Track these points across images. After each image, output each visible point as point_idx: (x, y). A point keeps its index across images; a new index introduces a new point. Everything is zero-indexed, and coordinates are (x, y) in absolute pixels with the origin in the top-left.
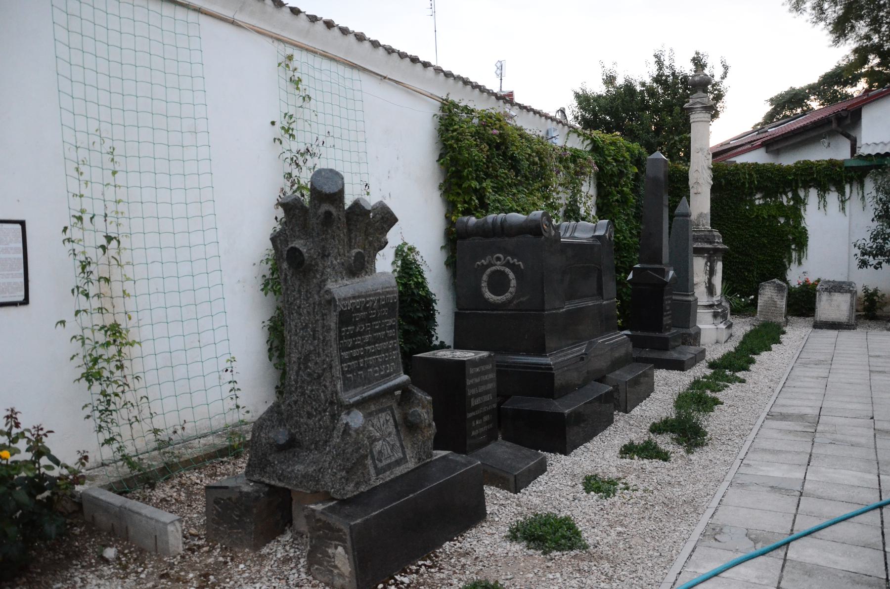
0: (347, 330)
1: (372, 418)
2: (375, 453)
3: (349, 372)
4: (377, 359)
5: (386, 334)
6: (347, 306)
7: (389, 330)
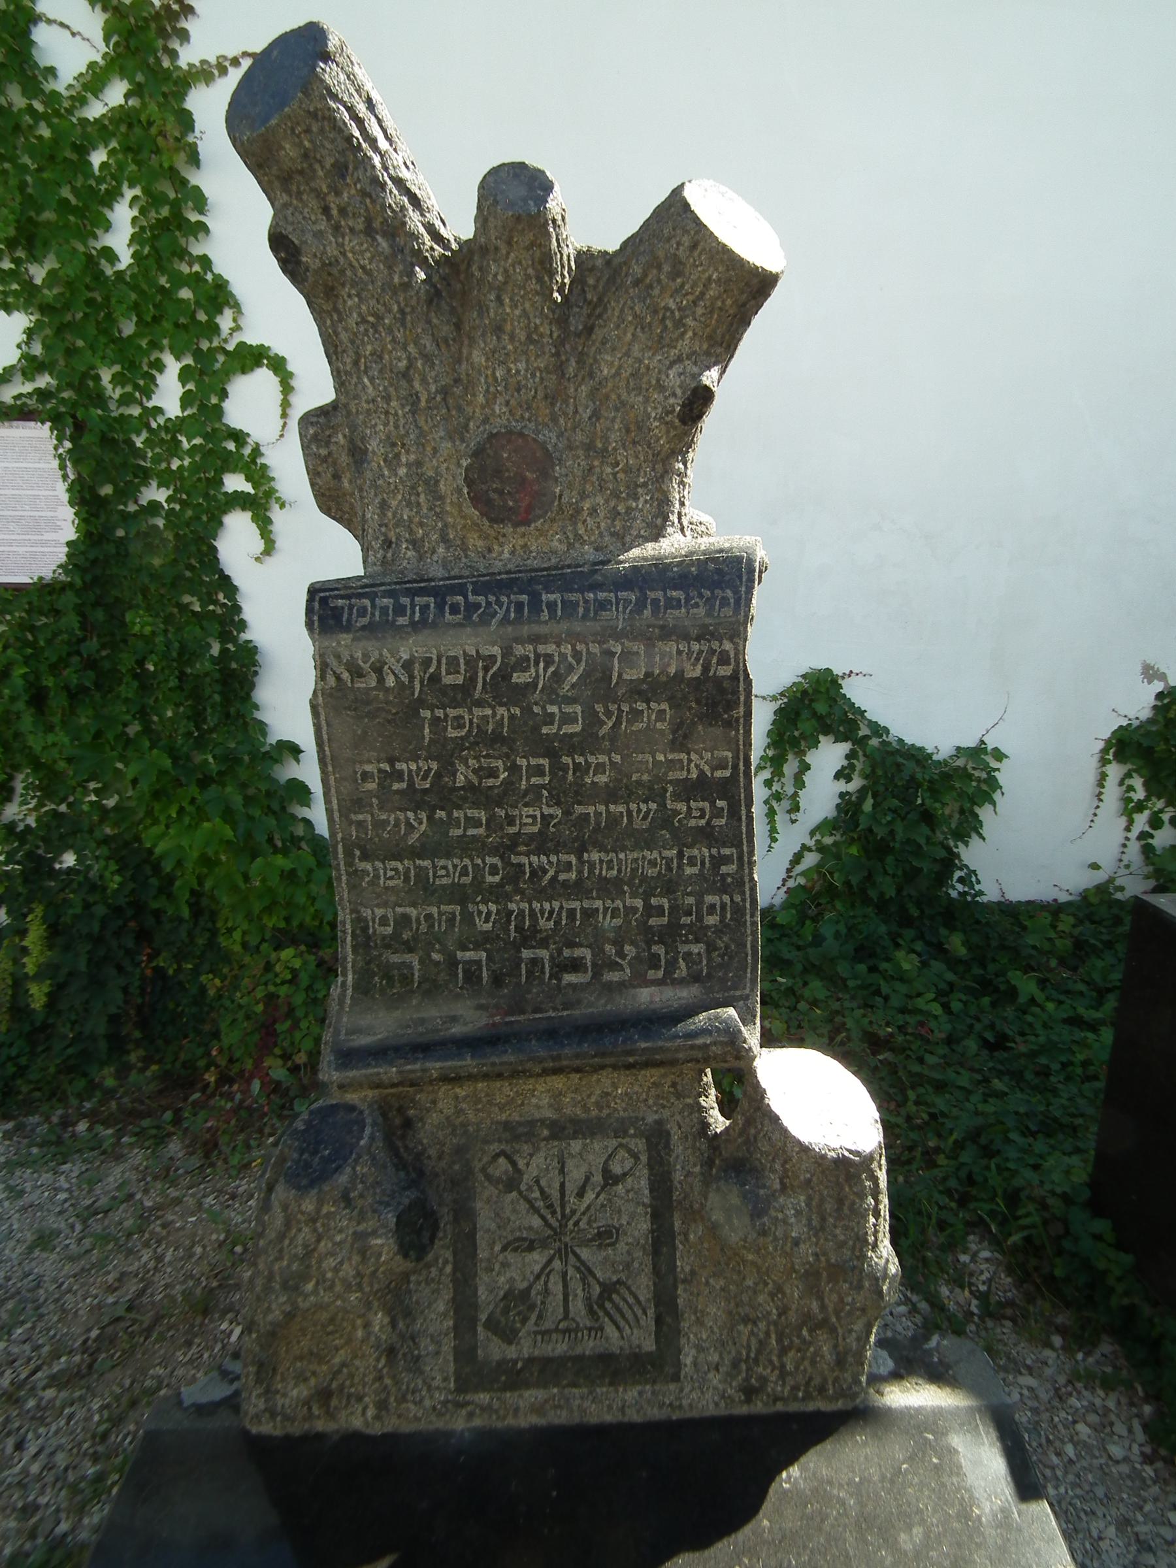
0: (399, 776)
1: (526, 1148)
2: (483, 1294)
3: (391, 943)
4: (589, 914)
5: (665, 820)
6: (378, 669)
7: (677, 797)
